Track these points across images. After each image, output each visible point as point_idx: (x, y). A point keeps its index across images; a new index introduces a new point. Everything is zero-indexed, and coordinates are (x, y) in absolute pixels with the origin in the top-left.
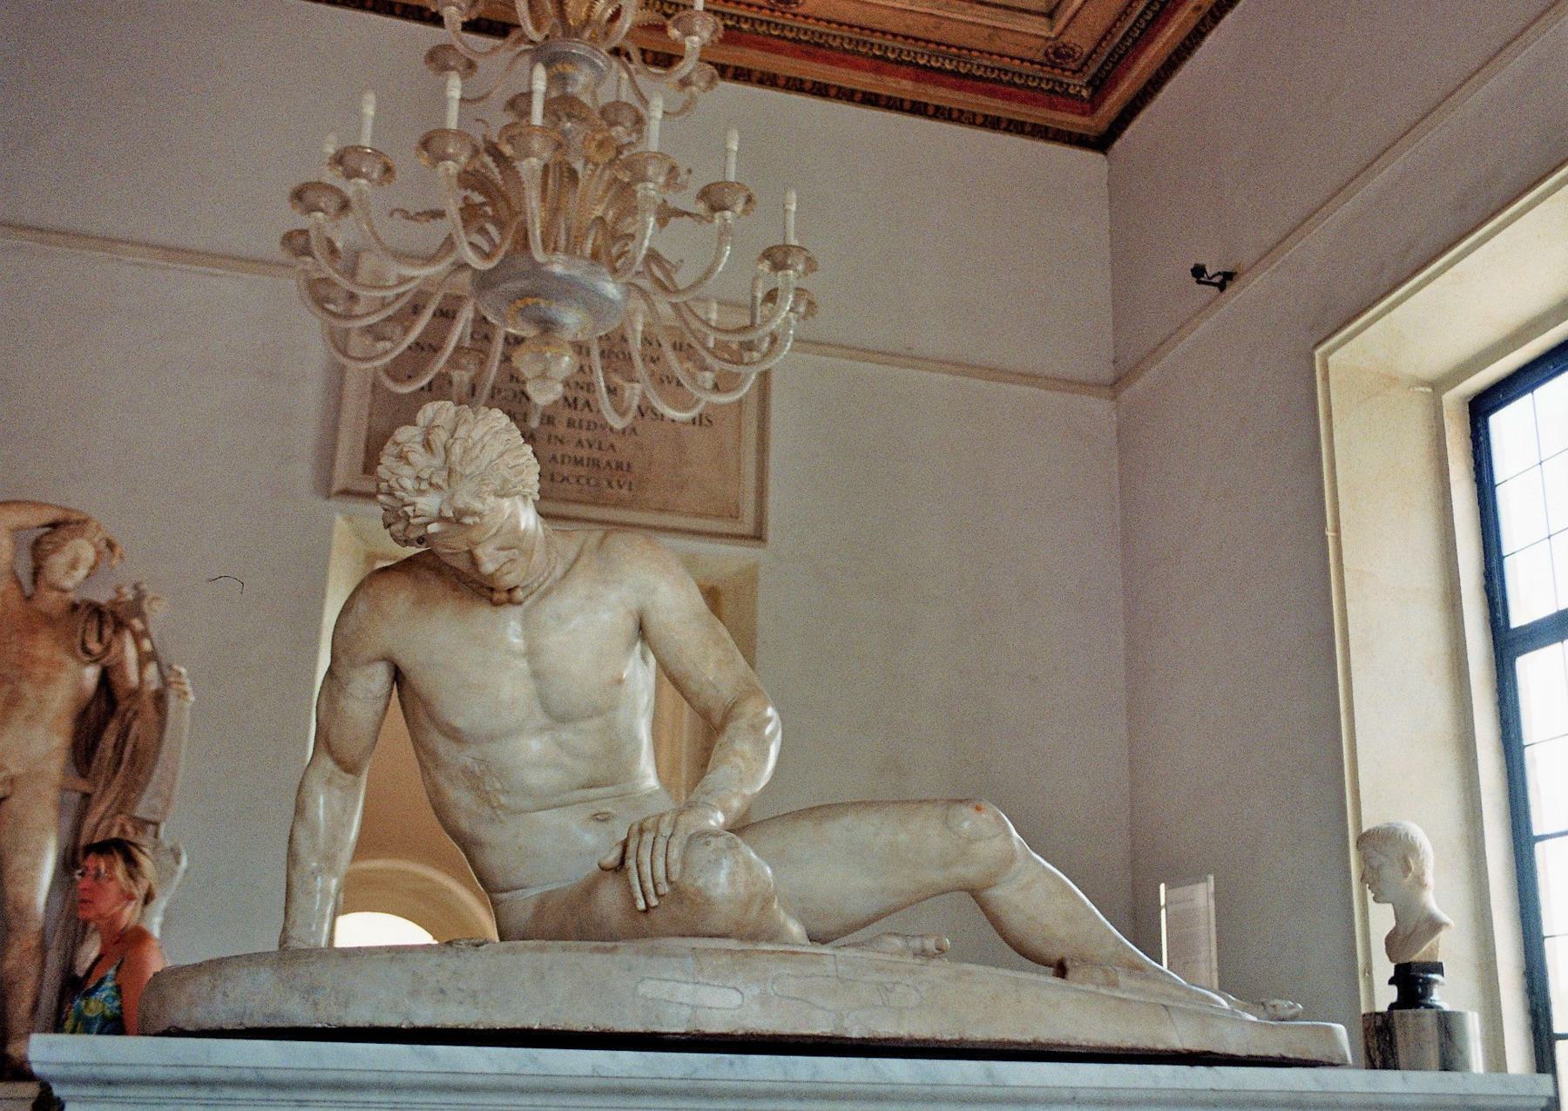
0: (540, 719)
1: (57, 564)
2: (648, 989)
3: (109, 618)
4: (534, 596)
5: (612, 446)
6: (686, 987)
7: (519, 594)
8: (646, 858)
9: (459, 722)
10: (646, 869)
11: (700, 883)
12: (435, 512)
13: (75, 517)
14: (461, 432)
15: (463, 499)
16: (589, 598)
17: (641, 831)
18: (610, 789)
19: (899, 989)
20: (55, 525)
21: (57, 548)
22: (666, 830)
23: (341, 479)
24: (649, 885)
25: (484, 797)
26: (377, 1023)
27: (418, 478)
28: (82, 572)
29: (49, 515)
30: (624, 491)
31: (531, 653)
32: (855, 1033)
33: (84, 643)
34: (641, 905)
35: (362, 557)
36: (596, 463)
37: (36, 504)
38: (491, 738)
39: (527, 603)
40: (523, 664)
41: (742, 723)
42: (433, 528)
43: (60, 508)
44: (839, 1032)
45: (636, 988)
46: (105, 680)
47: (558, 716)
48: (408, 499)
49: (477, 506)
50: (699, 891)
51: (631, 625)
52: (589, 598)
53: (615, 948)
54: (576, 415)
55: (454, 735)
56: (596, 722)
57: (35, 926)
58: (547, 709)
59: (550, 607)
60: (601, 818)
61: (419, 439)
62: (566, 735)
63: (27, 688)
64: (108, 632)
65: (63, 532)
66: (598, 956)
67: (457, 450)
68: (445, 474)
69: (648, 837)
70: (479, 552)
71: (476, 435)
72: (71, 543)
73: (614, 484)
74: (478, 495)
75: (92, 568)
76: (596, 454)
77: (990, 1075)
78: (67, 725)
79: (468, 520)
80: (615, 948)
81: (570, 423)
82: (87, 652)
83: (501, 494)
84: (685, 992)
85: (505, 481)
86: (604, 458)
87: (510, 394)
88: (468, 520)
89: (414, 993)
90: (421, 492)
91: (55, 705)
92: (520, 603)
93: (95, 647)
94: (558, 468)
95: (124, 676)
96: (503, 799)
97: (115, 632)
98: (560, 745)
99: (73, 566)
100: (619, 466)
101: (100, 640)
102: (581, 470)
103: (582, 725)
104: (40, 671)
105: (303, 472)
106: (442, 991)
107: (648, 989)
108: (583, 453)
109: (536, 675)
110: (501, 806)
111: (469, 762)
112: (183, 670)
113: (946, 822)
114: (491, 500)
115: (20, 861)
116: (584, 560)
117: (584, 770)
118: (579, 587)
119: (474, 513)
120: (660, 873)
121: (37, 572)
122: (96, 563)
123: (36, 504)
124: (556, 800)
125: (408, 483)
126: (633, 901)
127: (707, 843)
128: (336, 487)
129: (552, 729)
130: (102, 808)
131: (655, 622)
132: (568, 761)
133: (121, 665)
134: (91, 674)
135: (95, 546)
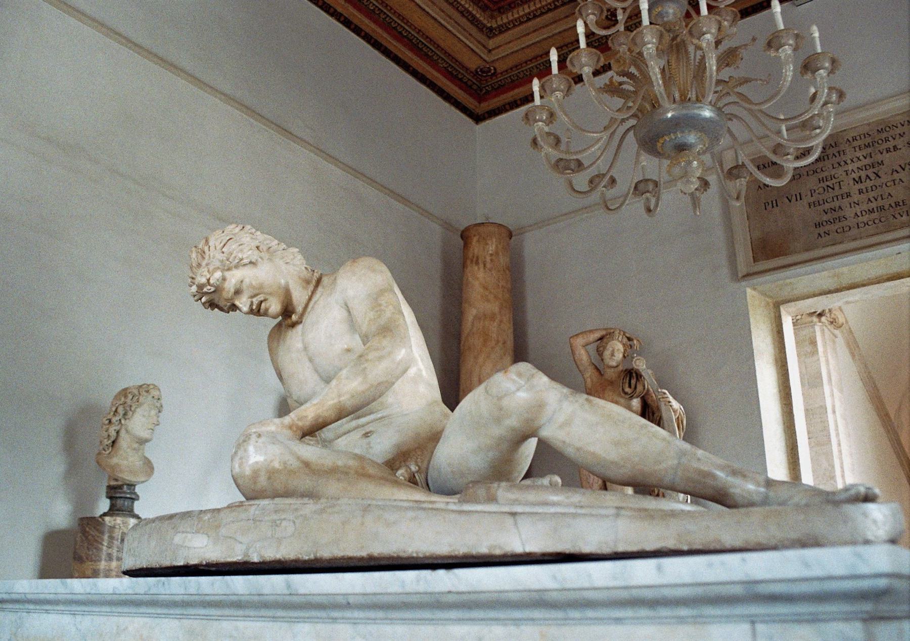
1: (607, 354)
2: (178, 539)
5: (890, 194)
19: (284, 523)
20: (601, 339)
21: (605, 348)
23: (742, 269)
29: (604, 333)
30: (905, 218)
31: (305, 348)
32: (255, 559)
33: (623, 390)
35: (772, 305)
36: (882, 208)
37: (591, 331)
43: (605, 329)
44: (246, 559)
54: (861, 186)
64: (633, 382)
65: (605, 340)
73: (897, 216)
76: (880, 202)
77: (289, 586)
81: (860, 192)
82: (626, 393)
86: (886, 203)
87: (821, 190)
93: (627, 390)
94: (860, 219)
97: (637, 379)
99: (613, 355)
100: (897, 204)
101: (630, 386)
102: (875, 215)
105: (725, 271)
108: (874, 205)
109: (311, 360)
123: (591, 331)
128: (740, 275)
135: (621, 342)
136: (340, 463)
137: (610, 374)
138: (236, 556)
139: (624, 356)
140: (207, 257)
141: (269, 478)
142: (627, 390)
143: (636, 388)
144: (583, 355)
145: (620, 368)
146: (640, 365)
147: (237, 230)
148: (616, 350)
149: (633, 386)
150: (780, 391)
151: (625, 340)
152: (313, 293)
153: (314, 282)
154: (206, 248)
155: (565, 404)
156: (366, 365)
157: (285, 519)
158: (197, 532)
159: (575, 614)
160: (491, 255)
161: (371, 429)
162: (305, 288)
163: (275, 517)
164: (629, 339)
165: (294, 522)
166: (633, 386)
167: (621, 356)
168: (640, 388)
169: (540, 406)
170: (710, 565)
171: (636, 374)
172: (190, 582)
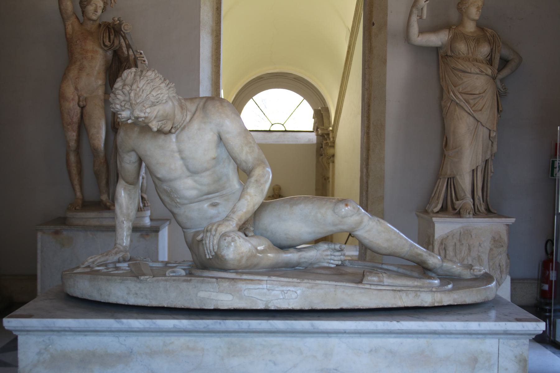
0: (188, 174)
1: (90, 9)
2: (202, 294)
3: (113, 31)
4: (180, 130)
6: (215, 294)
7: (173, 130)
8: (208, 242)
9: (159, 176)
10: (208, 245)
11: (223, 253)
12: (129, 116)
14: (134, 87)
15: (137, 113)
16: (199, 129)
17: (207, 231)
18: (217, 194)
22: (213, 233)
24: (209, 251)
25: (172, 199)
26: (118, 303)
27: (121, 106)
28: (100, 12)
34: (208, 257)
38: (171, 180)
39: (177, 132)
40: (177, 155)
41: (253, 179)
42: (130, 121)
44: (267, 308)
45: (197, 294)
46: (116, 54)
47: (193, 173)
48: (119, 113)
49: (142, 115)
50: (222, 256)
51: (216, 138)
52: (199, 129)
53: (191, 280)
55: (159, 179)
56: (208, 173)
57: (102, 154)
58: (188, 169)
59: (185, 135)
60: (214, 205)
61: (121, 88)
62: (197, 178)
63: (86, 63)
64: (112, 37)
66: (185, 283)
67: (132, 95)
68: (129, 103)
69: (209, 234)
70: (150, 125)
71: (141, 85)
74: (141, 111)
75: (103, 9)
78: (102, 75)
79: (140, 120)
80: (191, 280)
82: (105, 46)
83: (153, 105)
84: (214, 295)
85: (153, 102)
88: (140, 120)
89: (128, 294)
90: (123, 111)
91: (97, 68)
92: (174, 133)
93: (107, 43)
95: (123, 53)
96: (178, 200)
97: (115, 36)
98: (195, 181)
99: (96, 11)
101: (110, 41)
103: (202, 174)
104: (89, 55)
106: (137, 294)
107: (202, 294)
109: (182, 159)
110: (178, 202)
111: (165, 187)
112: (142, 52)
113: (334, 211)
114: (148, 110)
115: (93, 131)
116: (197, 114)
117: (205, 189)
118: (195, 125)
119: (141, 117)
120: (212, 249)
121: (83, 12)
122: (104, 7)
124: (196, 200)
125: (118, 106)
126: (205, 255)
127: (225, 240)
129: (191, 176)
131: (224, 136)
132: (199, 187)
133: (121, 47)
134: (110, 54)
137: (90, 26)
138: (261, 306)
139: (102, 12)
141: (247, 260)
142: (107, 43)
143: (113, 42)
145: (98, 22)
150: (212, 56)
155: (371, 222)
157: (289, 290)
158: (222, 292)
159: (448, 336)
161: (217, 201)
163: (281, 288)
165: (296, 292)
169: (361, 222)
170: (495, 325)
171: (114, 29)
172: (242, 323)
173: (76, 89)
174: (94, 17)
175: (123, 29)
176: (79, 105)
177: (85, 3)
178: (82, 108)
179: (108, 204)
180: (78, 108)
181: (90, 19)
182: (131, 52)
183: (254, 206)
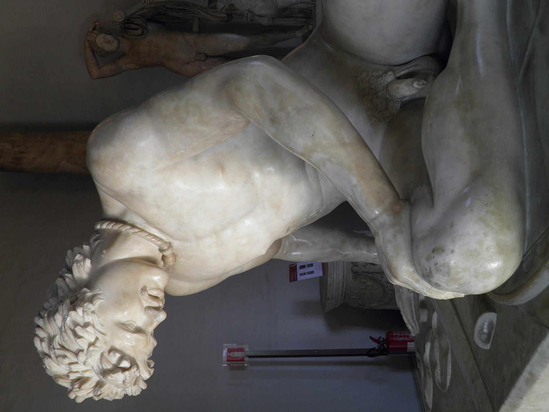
1: (107, 47)
3: (127, 25)
13: (87, 43)
16: (158, 207)
20: (93, 51)
28: (109, 37)
46: (150, 20)
52: (158, 207)
64: (133, 26)
72: (100, 45)
75: (107, 34)
82: (143, 34)
93: (139, 32)
97: (132, 23)
99: (109, 42)
101: (137, 29)
122: (104, 33)
130: (204, 14)
134: (151, 27)
136: (460, 131)
139: (110, 34)
140: (86, 375)
142: (139, 32)
144: (107, 69)
146: (119, 17)
147: (41, 334)
148: (103, 41)
149: (138, 27)
151: (96, 31)
152: (133, 226)
153: (117, 227)
154: (73, 377)
156: (290, 109)
160: (13, 147)
162: (127, 236)
164: (94, 29)
166: (138, 27)
167: (109, 36)
168: (138, 21)
173: (188, 63)
174: (115, 44)
175: (123, 19)
176: (205, 60)
177: (102, 52)
178: (207, 56)
179: (306, 31)
180: (208, 61)
181: (118, 47)
182: (148, 7)
183: (343, 144)
